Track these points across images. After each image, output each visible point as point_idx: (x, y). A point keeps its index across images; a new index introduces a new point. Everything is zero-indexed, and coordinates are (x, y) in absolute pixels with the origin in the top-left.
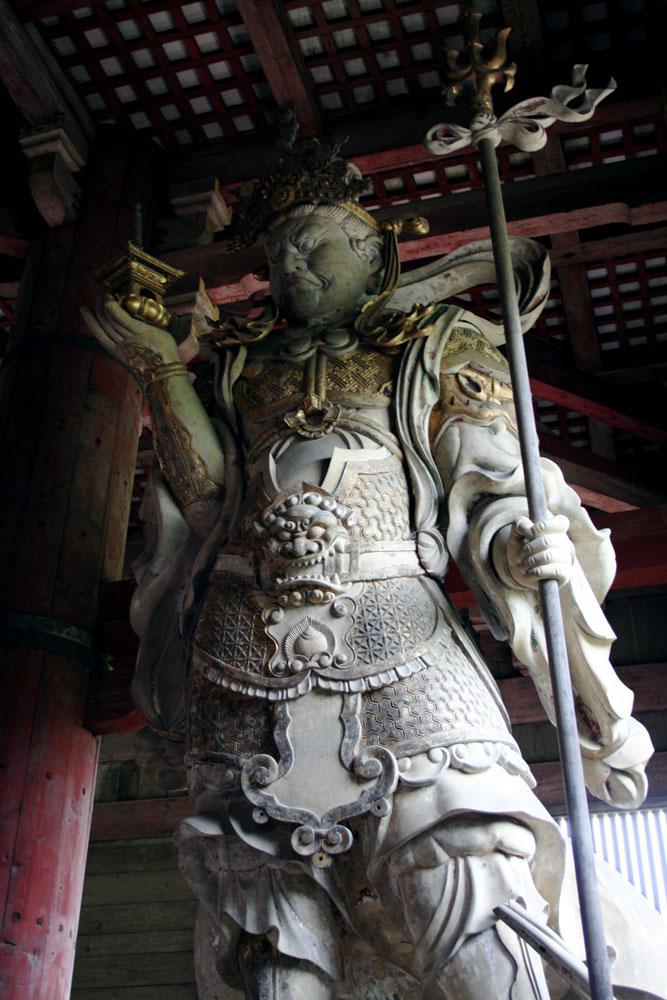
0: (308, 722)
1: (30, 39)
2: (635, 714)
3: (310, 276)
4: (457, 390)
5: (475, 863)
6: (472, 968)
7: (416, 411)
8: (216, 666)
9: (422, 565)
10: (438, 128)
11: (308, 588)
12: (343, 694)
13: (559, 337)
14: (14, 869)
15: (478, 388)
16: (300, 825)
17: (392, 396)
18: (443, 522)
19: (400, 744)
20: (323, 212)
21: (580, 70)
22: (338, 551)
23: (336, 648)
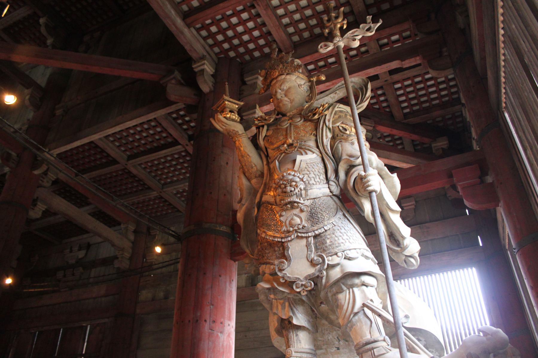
1: (192, 32)
2: (411, 236)
3: (286, 99)
4: (339, 132)
5: (355, 289)
7: (325, 140)
8: (264, 232)
9: (331, 192)
10: (322, 44)
11: (292, 203)
12: (307, 238)
13: (388, 110)
14: (212, 307)
15: (346, 130)
17: (316, 136)
20: (288, 77)
22: (301, 190)
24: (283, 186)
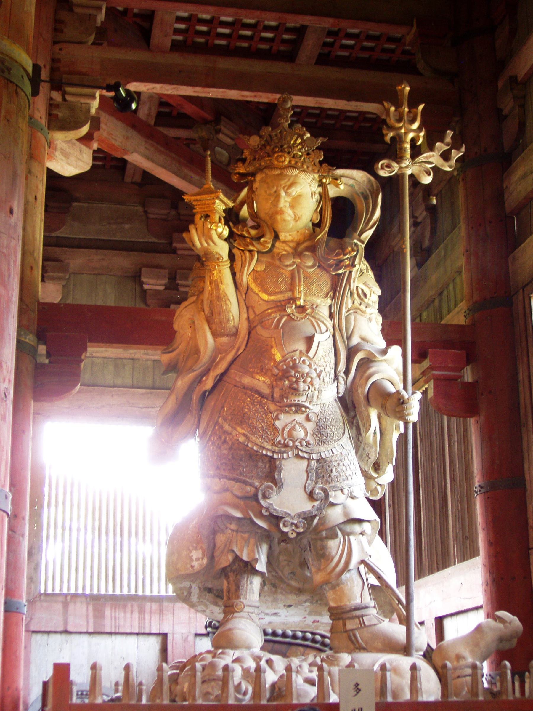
0: (293, 471)
3: (290, 211)
5: (352, 538)
6: (347, 583)
12: (309, 459)
16: (284, 518)
18: (347, 372)
19: (331, 485)
20: (303, 176)
21: (449, 134)
22: (315, 389)
23: (308, 437)
24: (294, 380)
